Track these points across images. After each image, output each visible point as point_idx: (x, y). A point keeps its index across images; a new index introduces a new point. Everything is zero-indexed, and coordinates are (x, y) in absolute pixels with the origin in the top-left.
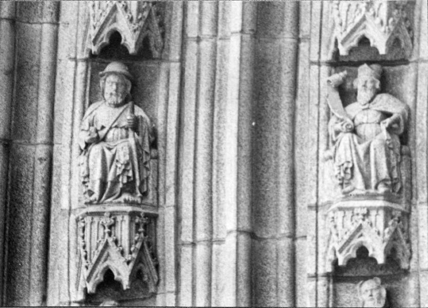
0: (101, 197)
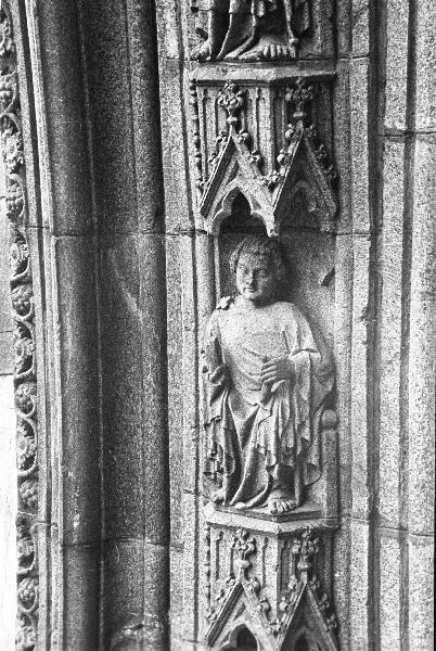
0: (217, 46)
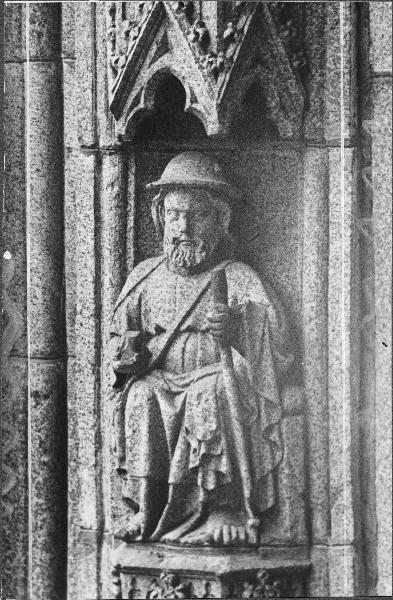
0: (151, 524)
